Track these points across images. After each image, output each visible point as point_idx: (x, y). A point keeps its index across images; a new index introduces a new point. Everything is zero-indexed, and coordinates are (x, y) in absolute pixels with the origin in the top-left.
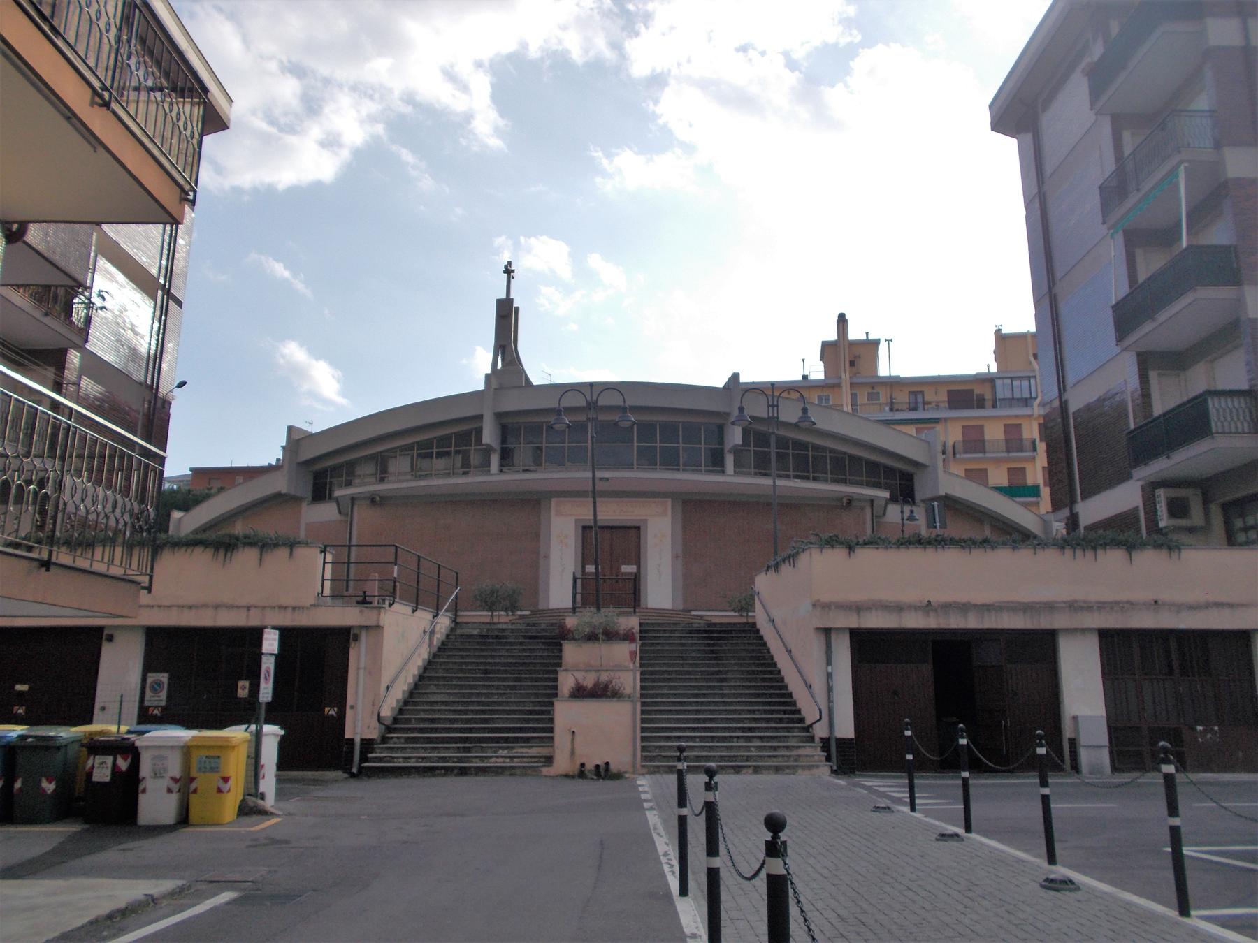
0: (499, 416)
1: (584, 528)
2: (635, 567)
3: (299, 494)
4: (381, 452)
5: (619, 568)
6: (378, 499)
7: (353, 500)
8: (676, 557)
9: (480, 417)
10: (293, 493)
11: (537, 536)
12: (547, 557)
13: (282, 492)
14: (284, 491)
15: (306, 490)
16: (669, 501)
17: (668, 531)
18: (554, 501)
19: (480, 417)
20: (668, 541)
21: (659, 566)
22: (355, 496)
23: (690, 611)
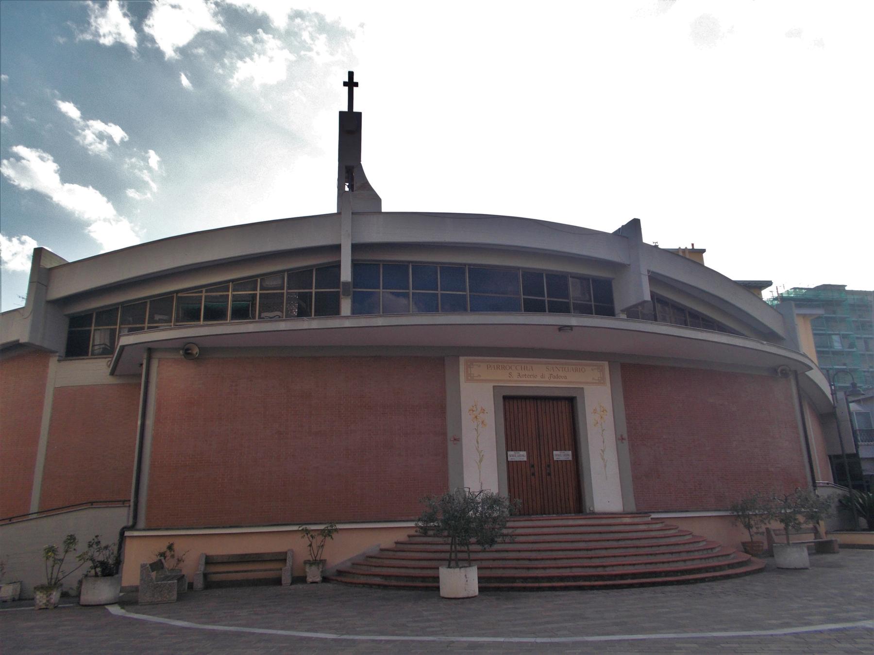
0: (356, 248)
1: (505, 398)
2: (570, 453)
3: (46, 345)
4: (177, 292)
5: (550, 456)
6: (196, 351)
7: (151, 350)
8: (620, 439)
9: (336, 249)
10: (38, 343)
11: (443, 408)
12: (457, 440)
13: (22, 341)
14: (24, 339)
15: (58, 340)
16: (606, 364)
17: (608, 405)
18: (462, 360)
19: (336, 249)
20: (609, 417)
21: (603, 451)
22: (150, 345)
23: (647, 513)
